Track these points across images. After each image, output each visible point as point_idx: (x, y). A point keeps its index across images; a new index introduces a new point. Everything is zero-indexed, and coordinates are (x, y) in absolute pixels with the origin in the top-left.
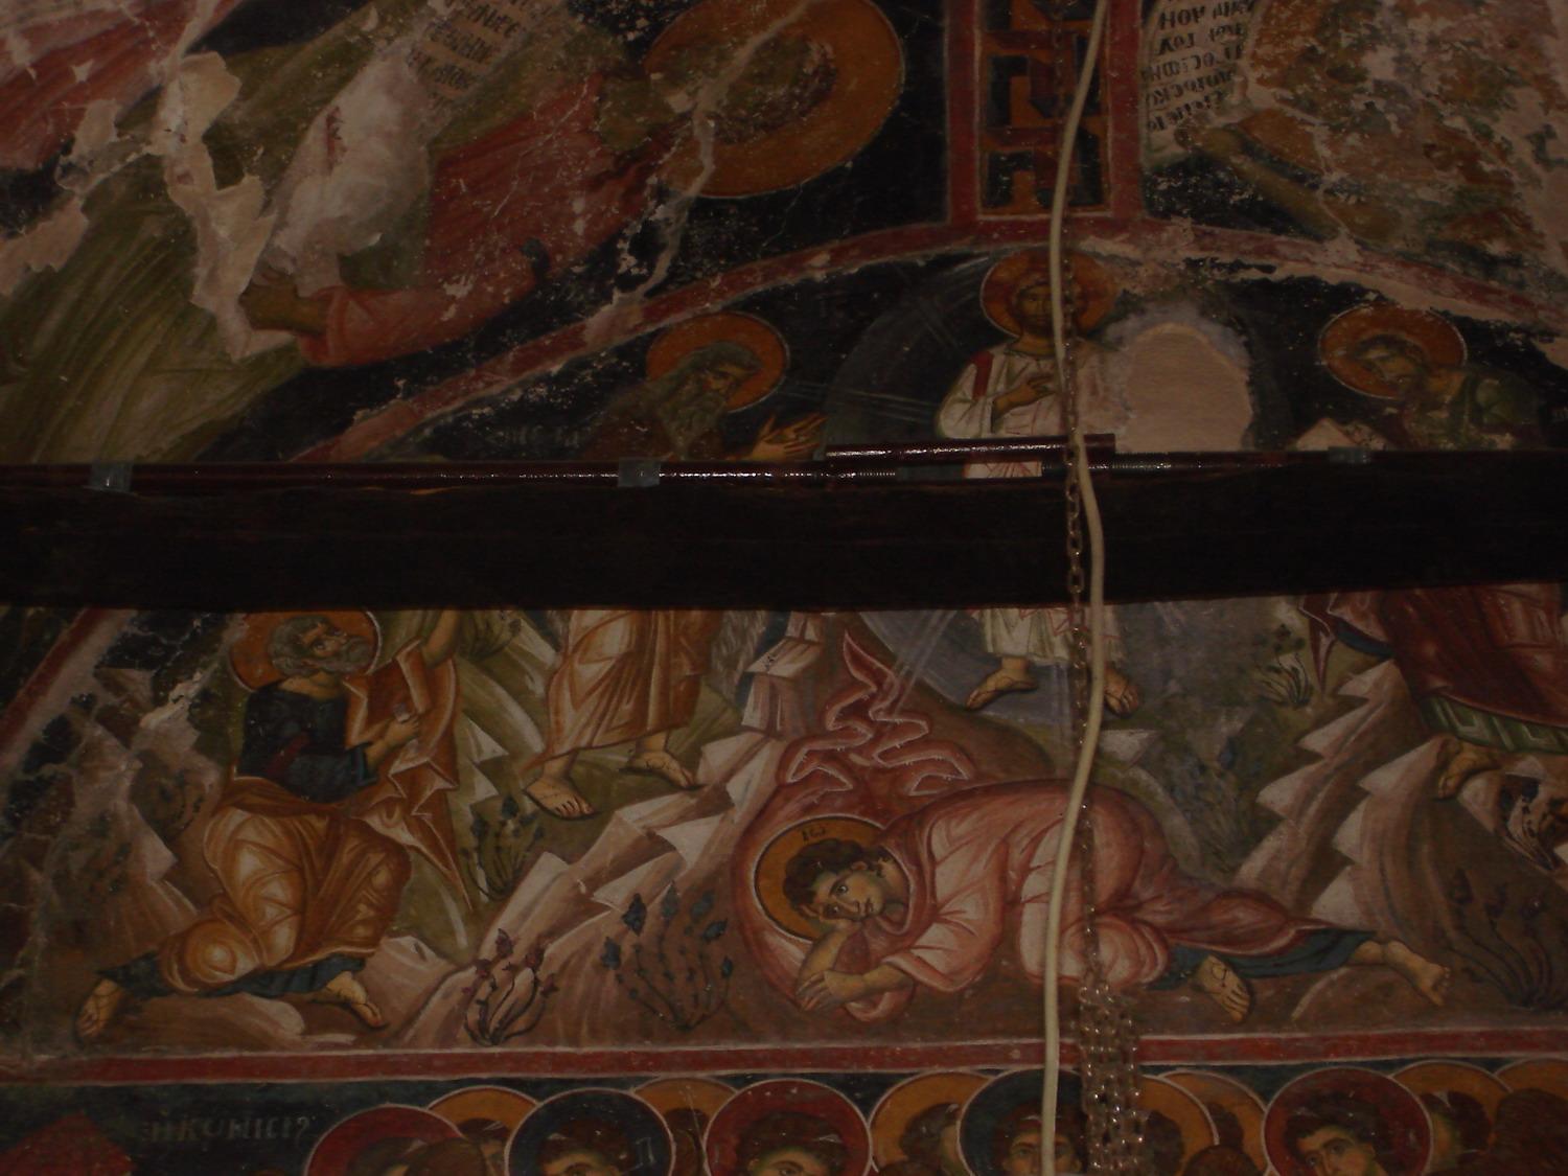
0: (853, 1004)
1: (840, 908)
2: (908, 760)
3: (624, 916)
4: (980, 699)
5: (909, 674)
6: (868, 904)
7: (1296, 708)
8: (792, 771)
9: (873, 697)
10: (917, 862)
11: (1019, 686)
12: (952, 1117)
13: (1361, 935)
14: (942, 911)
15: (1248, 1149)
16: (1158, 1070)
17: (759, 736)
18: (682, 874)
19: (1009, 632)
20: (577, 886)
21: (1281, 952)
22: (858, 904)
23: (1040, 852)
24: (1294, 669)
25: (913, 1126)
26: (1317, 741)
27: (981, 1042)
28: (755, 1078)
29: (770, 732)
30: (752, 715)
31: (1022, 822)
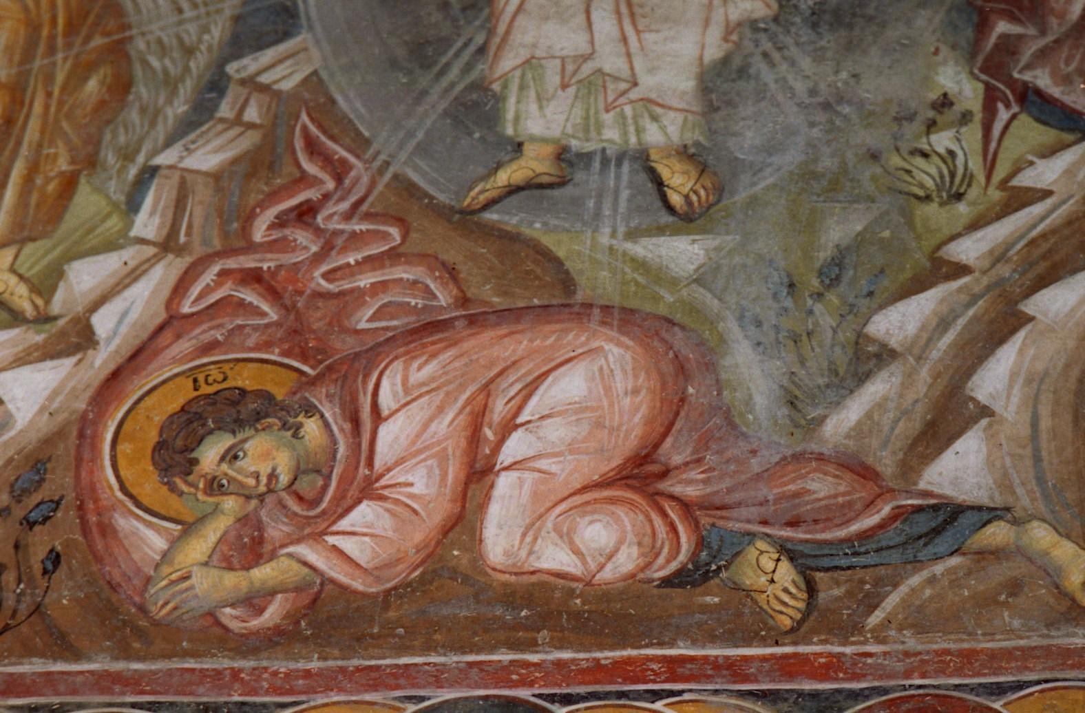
0: (228, 610)
1: (231, 480)
2: (365, 281)
4: (482, 198)
5: (387, 164)
6: (273, 476)
7: (942, 204)
8: (193, 298)
9: (326, 197)
10: (356, 422)
11: (545, 179)
13: (989, 514)
14: (383, 482)
16: (656, 695)
17: (151, 251)
19: (541, 108)
21: (864, 536)
22: (257, 476)
23: (534, 400)
24: (951, 153)
26: (969, 250)
29: (168, 245)
30: (148, 223)
31: (514, 363)
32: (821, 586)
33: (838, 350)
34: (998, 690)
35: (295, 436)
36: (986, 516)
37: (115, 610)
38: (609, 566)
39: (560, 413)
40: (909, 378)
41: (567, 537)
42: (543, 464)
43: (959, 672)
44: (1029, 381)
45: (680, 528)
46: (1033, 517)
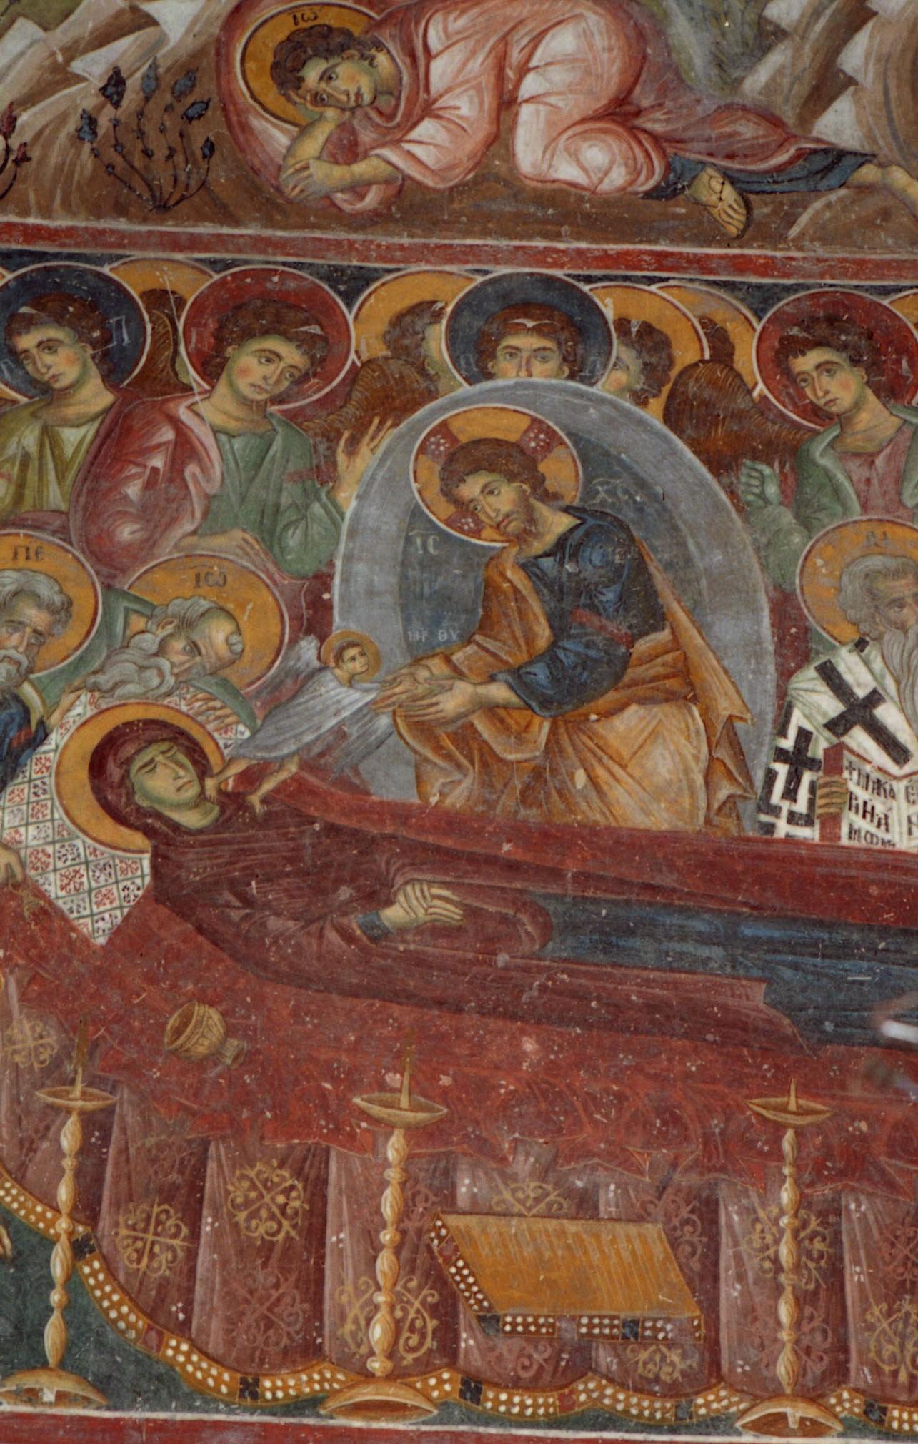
0: (339, 195)
1: (330, 95)
3: (103, 89)
6: (359, 95)
12: (437, 316)
13: (863, 158)
14: (437, 105)
15: (739, 364)
16: (651, 280)
18: (164, 50)
20: (53, 54)
21: (780, 169)
25: (397, 321)
27: (469, 242)
28: (234, 263)
32: (754, 205)
33: (746, 28)
34: (885, 291)
35: (371, 64)
36: (860, 160)
37: (259, 189)
38: (606, 181)
39: (558, 62)
40: (798, 51)
41: (575, 156)
42: (552, 100)
43: (856, 276)
44: (878, 61)
45: (653, 155)
46: (891, 163)
